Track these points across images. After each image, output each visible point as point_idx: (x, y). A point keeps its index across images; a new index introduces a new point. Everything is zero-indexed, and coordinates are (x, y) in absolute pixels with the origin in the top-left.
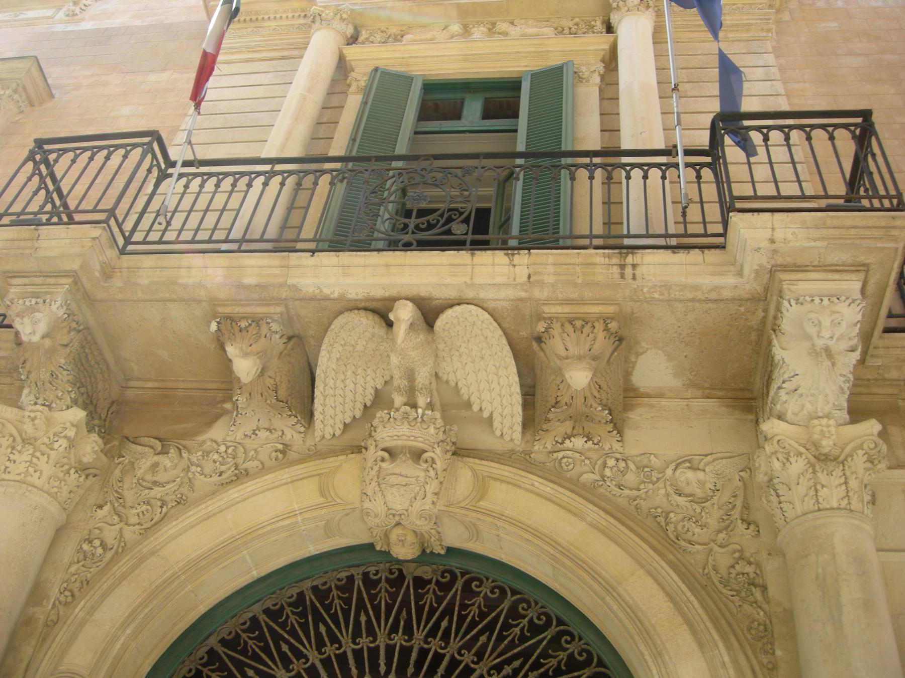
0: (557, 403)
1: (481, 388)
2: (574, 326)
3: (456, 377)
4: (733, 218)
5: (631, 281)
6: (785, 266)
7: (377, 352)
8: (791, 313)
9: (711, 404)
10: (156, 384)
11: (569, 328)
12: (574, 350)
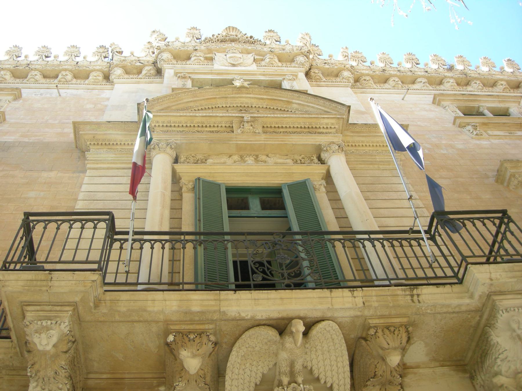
0: (375, 375)
1: (326, 369)
2: (390, 330)
3: (312, 364)
4: (471, 268)
5: (418, 304)
6: (495, 292)
7: (267, 351)
8: (502, 318)
9: (445, 369)
10: (109, 376)
11: (387, 332)
12: (392, 344)
